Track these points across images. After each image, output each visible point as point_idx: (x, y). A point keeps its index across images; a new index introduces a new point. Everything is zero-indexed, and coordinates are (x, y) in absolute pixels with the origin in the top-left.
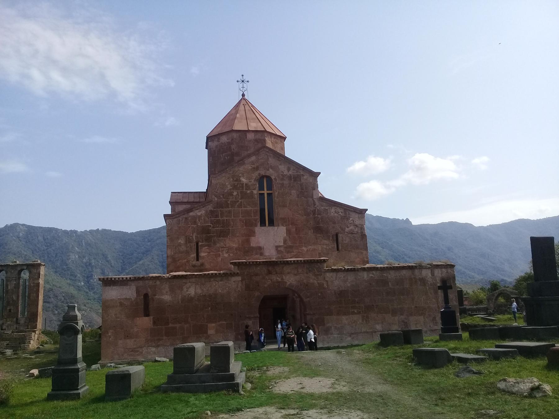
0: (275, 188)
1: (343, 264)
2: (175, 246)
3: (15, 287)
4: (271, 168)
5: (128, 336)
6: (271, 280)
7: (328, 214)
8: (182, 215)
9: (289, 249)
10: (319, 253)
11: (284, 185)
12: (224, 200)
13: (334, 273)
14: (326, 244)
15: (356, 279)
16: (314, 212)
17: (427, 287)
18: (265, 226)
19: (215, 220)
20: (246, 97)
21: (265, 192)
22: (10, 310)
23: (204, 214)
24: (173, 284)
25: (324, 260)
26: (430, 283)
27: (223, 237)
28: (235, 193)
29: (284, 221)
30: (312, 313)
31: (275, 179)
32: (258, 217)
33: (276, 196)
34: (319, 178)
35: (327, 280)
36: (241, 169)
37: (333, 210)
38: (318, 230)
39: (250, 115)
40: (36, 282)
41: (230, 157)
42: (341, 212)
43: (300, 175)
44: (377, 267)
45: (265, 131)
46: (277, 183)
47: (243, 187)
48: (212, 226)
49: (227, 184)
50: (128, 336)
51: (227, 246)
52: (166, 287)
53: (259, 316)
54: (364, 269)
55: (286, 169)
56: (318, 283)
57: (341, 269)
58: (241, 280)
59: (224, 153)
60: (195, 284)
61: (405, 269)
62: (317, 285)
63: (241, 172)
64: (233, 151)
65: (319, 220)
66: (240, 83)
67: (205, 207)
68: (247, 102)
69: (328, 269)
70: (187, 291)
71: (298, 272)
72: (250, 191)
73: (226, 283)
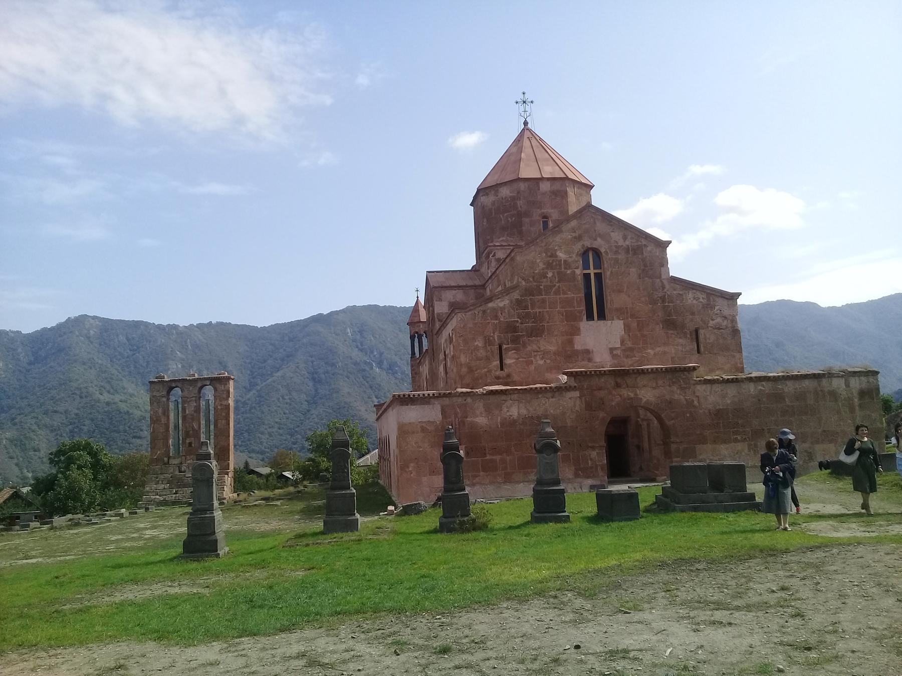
0: (606, 266)
1: (717, 373)
2: (470, 351)
3: (195, 411)
4: (600, 236)
6: (620, 396)
7: (684, 302)
8: (478, 307)
9: (629, 352)
10: (672, 358)
11: (618, 260)
12: (534, 284)
13: (708, 385)
15: (738, 393)
16: (663, 299)
17: (840, 404)
19: (523, 312)
20: (529, 126)
21: (592, 271)
22: (190, 444)
23: (507, 305)
24: (489, 401)
25: (694, 368)
26: (845, 398)
28: (550, 275)
29: (621, 313)
30: (678, 441)
31: (606, 252)
32: (583, 308)
33: (608, 277)
34: (670, 250)
35: (698, 395)
36: (558, 239)
37: (690, 295)
38: (671, 324)
39: (540, 154)
40: (224, 403)
41: (515, 220)
42: (703, 298)
43: (642, 245)
44: (768, 376)
45: (567, 178)
46: (609, 259)
47: (560, 265)
48: (519, 321)
49: (538, 261)
50: (434, 472)
51: (542, 349)
52: (479, 406)
53: (605, 445)
55: (621, 237)
56: (686, 400)
57: (718, 379)
58: (579, 396)
59: (506, 213)
60: (518, 402)
61: (808, 379)
62: (685, 403)
63: (557, 243)
64: (520, 209)
65: (671, 310)
66: (520, 104)
67: (509, 295)
68: (532, 133)
69: (700, 381)
70: (508, 411)
71: (657, 384)
72: (571, 270)
73: (559, 400)
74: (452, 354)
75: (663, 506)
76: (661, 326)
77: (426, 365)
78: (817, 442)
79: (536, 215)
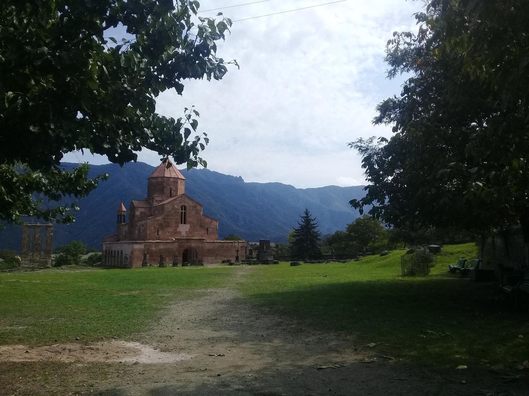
3: (40, 237)
4: (186, 202)
9: (190, 232)
14: (203, 232)
18: (182, 224)
21: (183, 211)
22: (37, 248)
27: (168, 227)
28: (172, 211)
32: (180, 221)
36: (175, 202)
37: (207, 219)
38: (201, 226)
40: (50, 234)
52: (154, 245)
74: (143, 229)
75: (191, 265)
76: (199, 227)
77: (126, 227)
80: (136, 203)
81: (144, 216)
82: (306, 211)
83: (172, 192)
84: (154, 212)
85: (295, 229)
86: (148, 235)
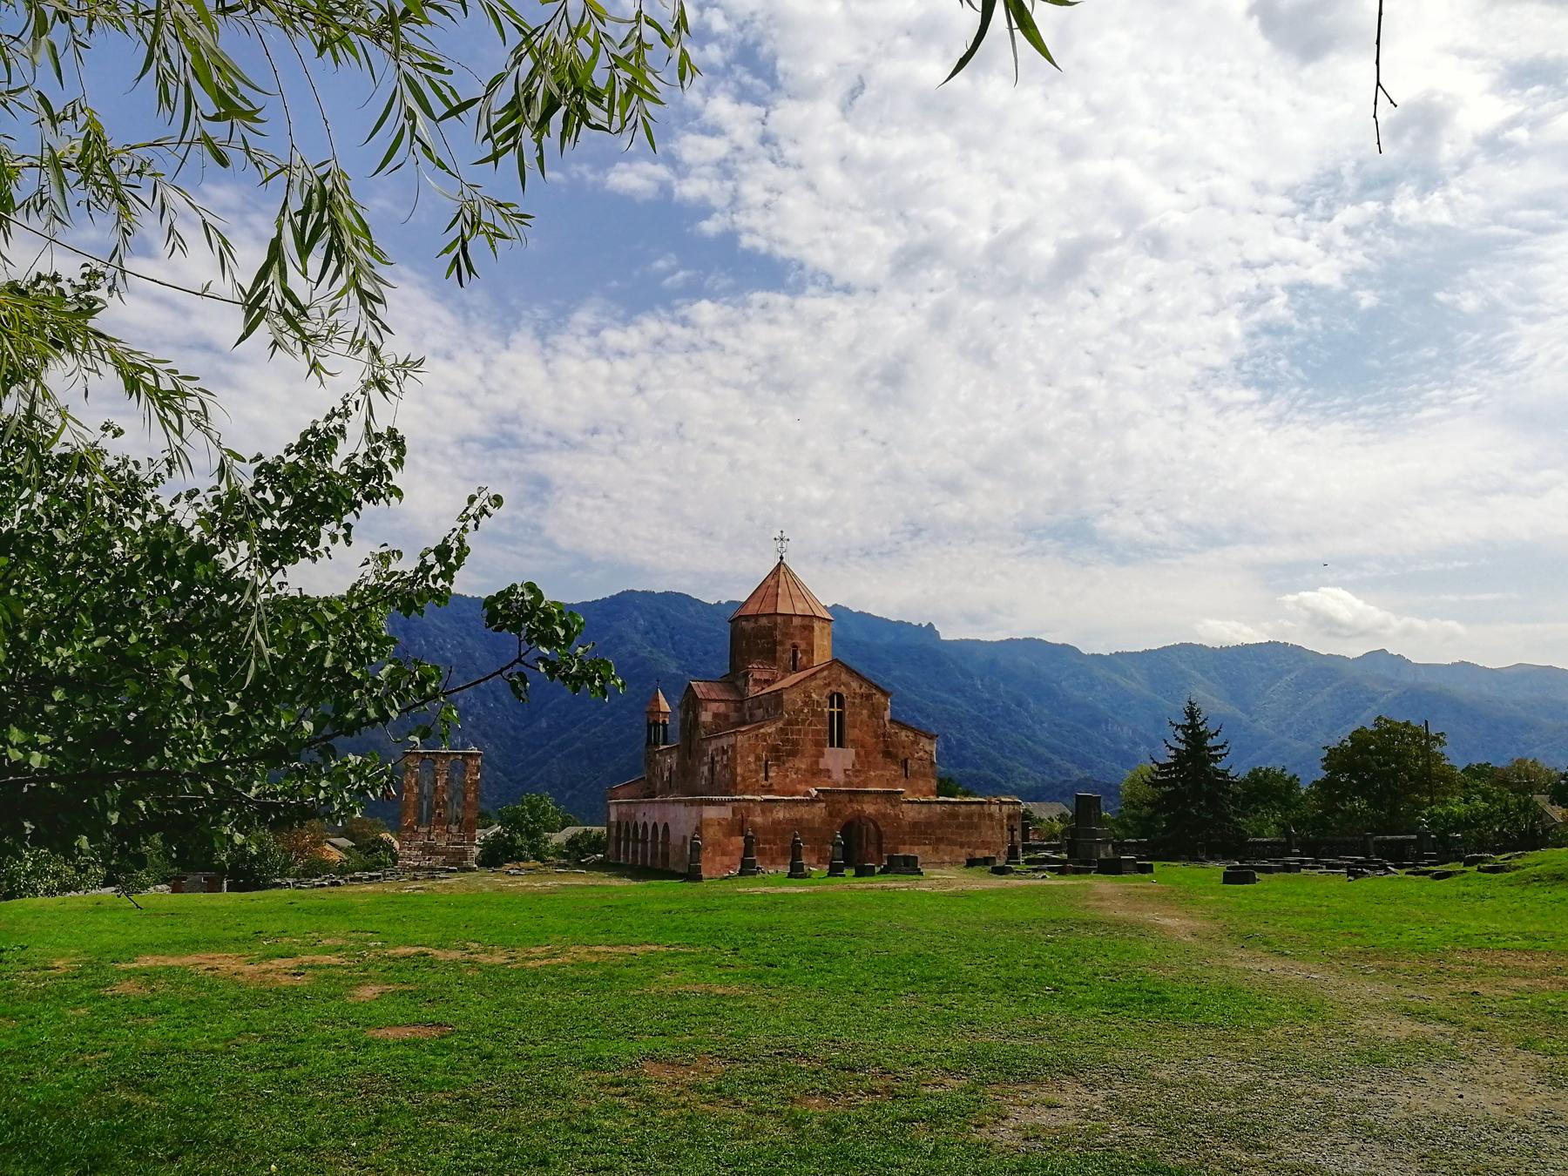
3: (447, 784)
5: (724, 854)
9: (857, 772)
14: (893, 770)
21: (836, 710)
22: (440, 814)
25: (902, 792)
28: (806, 711)
36: (813, 684)
37: (903, 734)
38: (887, 754)
39: (794, 591)
40: (474, 778)
45: (815, 616)
52: (758, 809)
54: (938, 802)
75: (882, 872)
78: (978, 848)
79: (788, 646)
80: (700, 688)
81: (723, 724)
82: (1191, 709)
83: (800, 656)
84: (751, 715)
85: (1158, 764)
86: (739, 779)
